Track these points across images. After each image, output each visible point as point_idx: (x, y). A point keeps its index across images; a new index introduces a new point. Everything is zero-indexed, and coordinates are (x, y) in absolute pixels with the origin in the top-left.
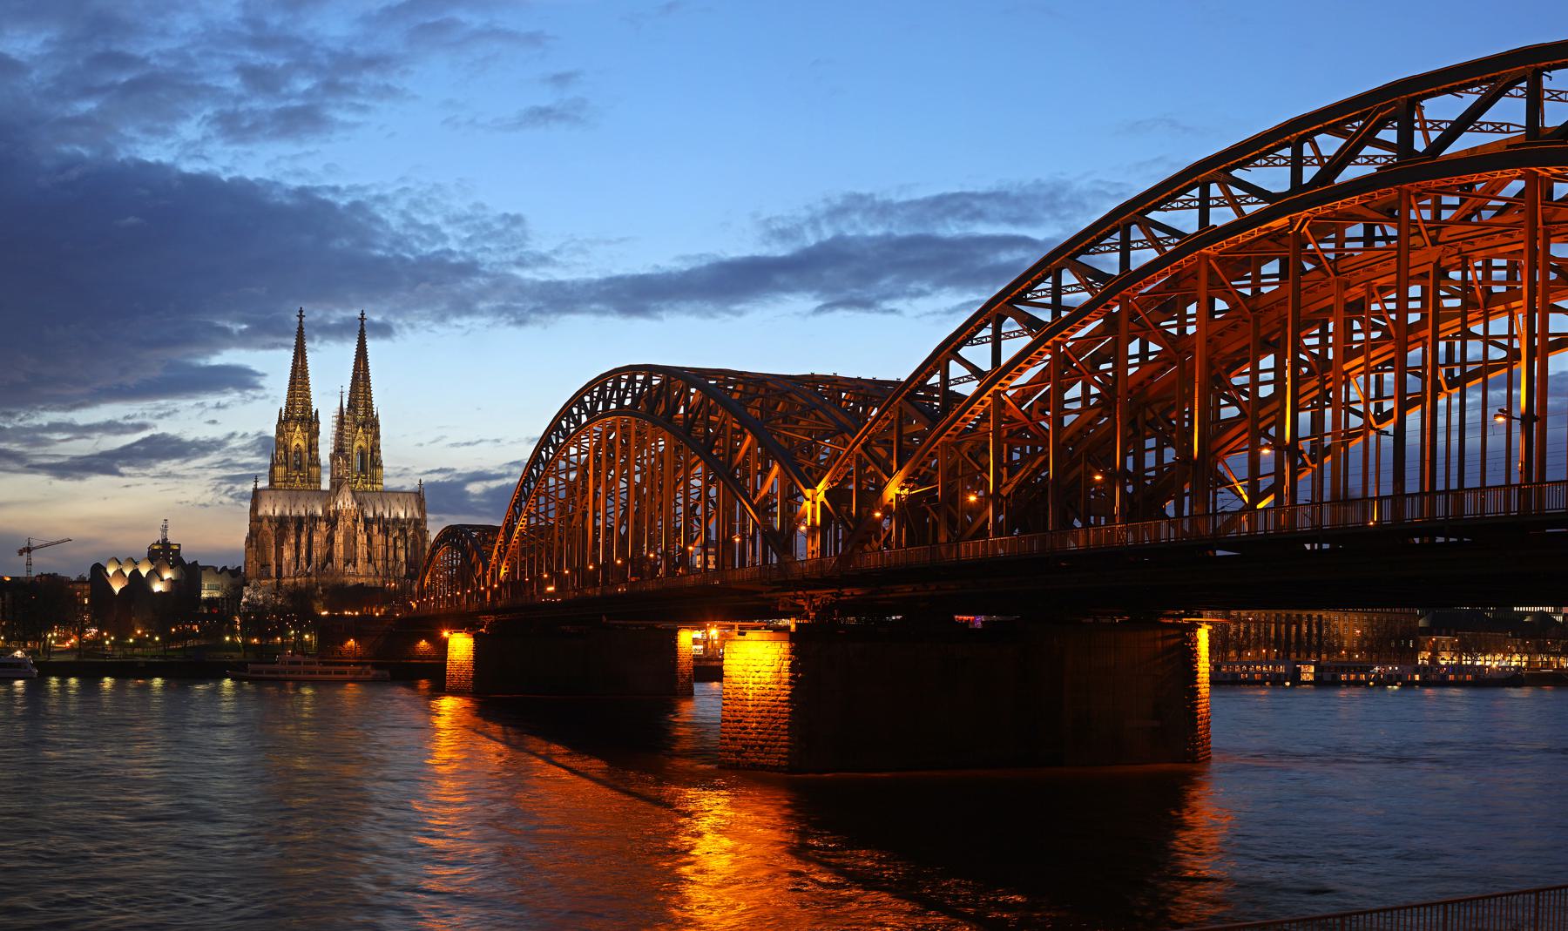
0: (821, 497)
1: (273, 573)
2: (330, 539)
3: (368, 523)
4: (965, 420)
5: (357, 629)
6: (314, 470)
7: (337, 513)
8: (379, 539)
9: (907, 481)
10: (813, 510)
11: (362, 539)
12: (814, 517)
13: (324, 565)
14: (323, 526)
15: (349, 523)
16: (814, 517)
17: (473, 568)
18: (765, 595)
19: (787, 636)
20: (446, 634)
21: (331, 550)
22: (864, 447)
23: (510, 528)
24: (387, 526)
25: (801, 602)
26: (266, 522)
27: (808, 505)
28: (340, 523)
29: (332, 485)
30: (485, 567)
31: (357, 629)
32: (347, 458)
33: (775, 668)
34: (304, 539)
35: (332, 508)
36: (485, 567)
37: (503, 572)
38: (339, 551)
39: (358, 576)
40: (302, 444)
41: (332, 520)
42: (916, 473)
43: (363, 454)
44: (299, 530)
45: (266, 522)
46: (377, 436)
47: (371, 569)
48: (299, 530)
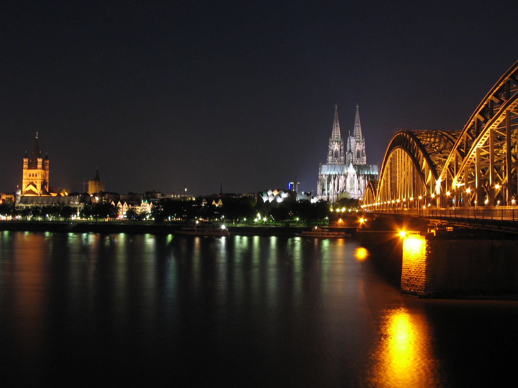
2: (345, 181)
7: (347, 173)
8: (362, 181)
11: (356, 181)
13: (343, 191)
14: (343, 177)
15: (352, 176)
19: (425, 237)
26: (324, 176)
28: (348, 176)
31: (344, 216)
38: (348, 186)
41: (346, 176)
42: (460, 178)
43: (358, 152)
44: (335, 179)
45: (324, 176)
47: (359, 191)
48: (335, 179)
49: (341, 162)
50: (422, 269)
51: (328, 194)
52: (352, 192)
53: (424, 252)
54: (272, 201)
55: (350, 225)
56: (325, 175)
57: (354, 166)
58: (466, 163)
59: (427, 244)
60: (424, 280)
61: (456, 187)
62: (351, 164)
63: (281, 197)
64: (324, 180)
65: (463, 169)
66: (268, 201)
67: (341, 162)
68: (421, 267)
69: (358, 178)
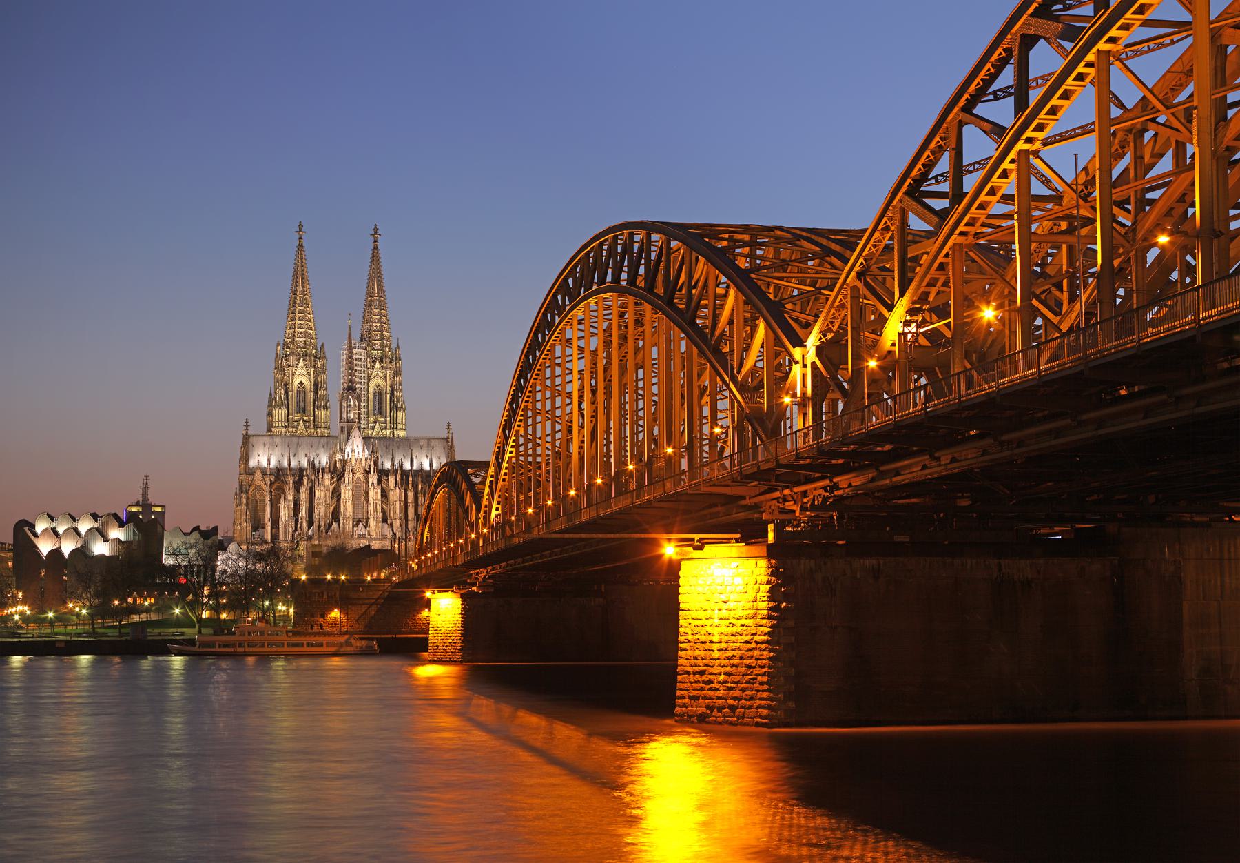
0: (811, 356)
1: (268, 537)
2: (336, 495)
3: (382, 474)
4: (982, 207)
5: (344, 597)
6: (322, 413)
7: (344, 462)
8: (395, 494)
9: (912, 311)
10: (804, 376)
11: (375, 493)
12: (804, 386)
14: (327, 477)
15: (359, 475)
16: (804, 386)
17: (467, 512)
18: (747, 502)
19: (765, 548)
20: (428, 594)
21: (338, 507)
22: (860, 275)
23: (500, 454)
24: (406, 478)
25: (790, 505)
26: (258, 474)
27: (797, 370)
29: (342, 429)
30: (478, 511)
32: (359, 398)
33: (750, 597)
34: (304, 495)
35: (338, 457)
36: (478, 511)
37: (494, 512)
38: (347, 509)
39: (371, 539)
40: (306, 382)
41: (338, 473)
42: (924, 298)
43: (380, 394)
44: (297, 487)
45: (258, 474)
46: (397, 373)
48: (297, 487)
49: (316, 427)
50: (757, 671)
51: (275, 537)
52: (360, 530)
53: (764, 605)
54: (73, 552)
55: (369, 628)
56: (264, 474)
57: (367, 440)
58: (961, 228)
59: (772, 574)
60: (765, 712)
61: (902, 335)
62: (356, 432)
63: (106, 540)
64: (259, 488)
65: (941, 259)
66: (56, 553)
67: (316, 427)
68: (752, 662)
69: (379, 482)
